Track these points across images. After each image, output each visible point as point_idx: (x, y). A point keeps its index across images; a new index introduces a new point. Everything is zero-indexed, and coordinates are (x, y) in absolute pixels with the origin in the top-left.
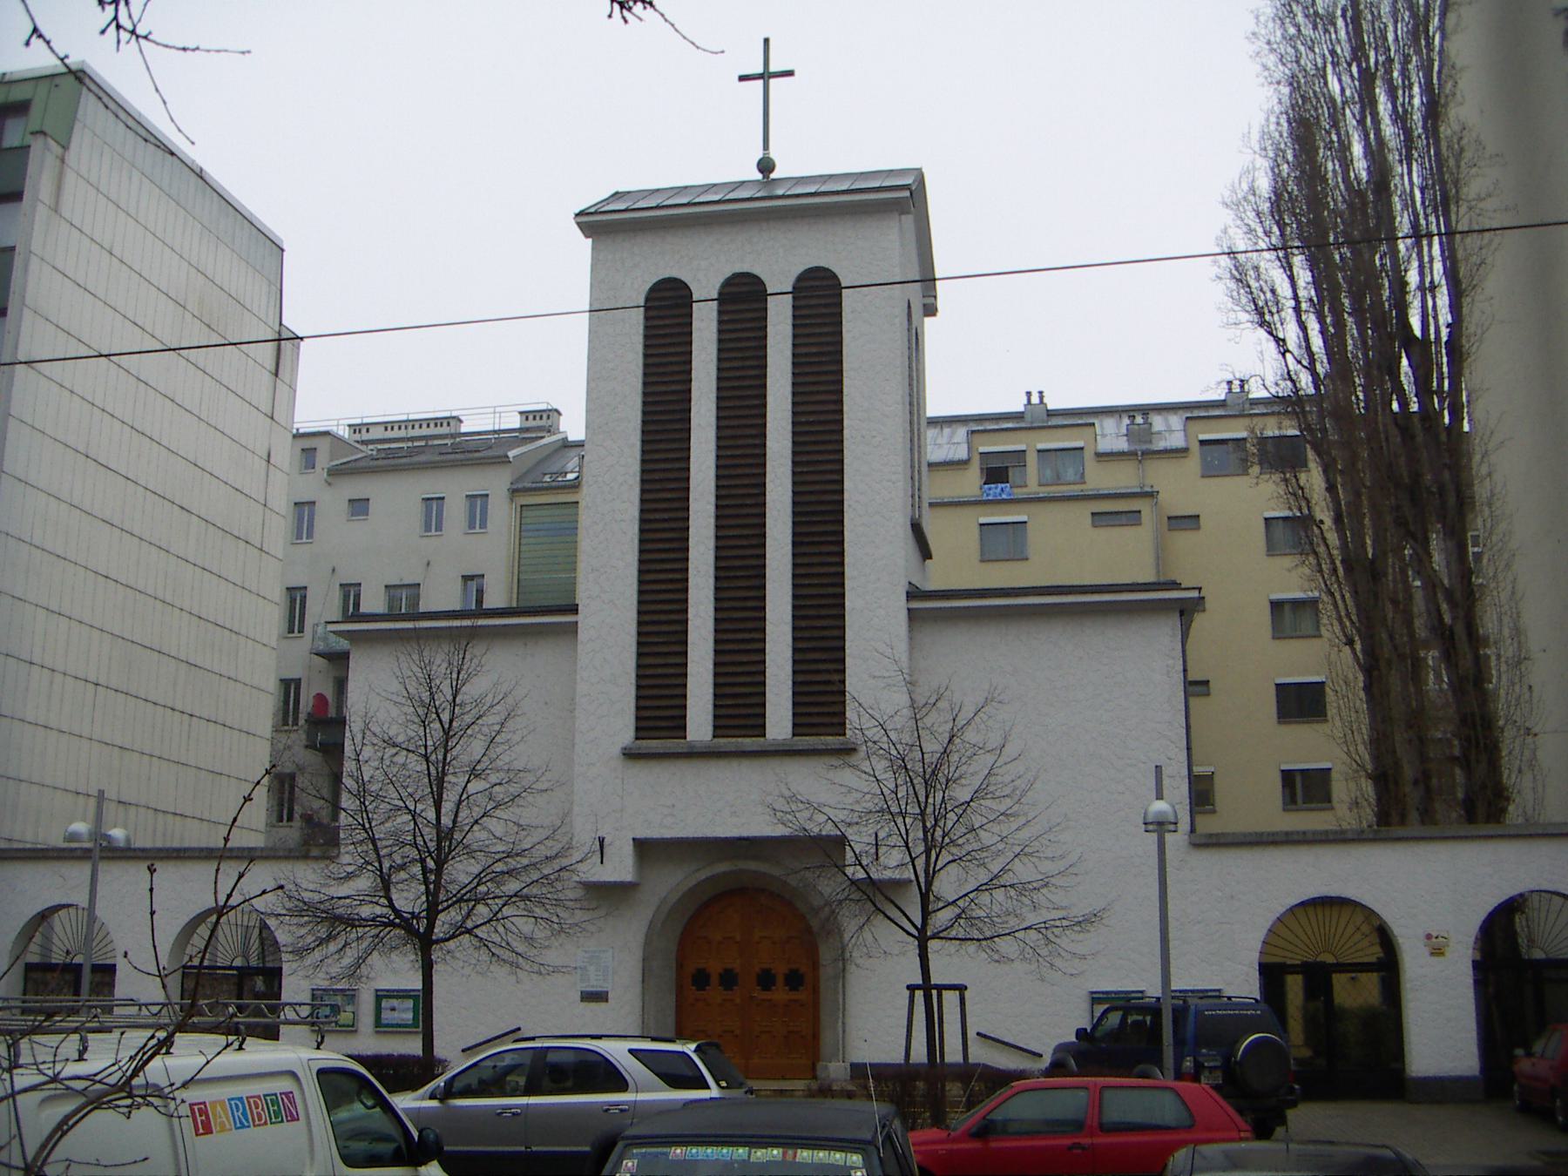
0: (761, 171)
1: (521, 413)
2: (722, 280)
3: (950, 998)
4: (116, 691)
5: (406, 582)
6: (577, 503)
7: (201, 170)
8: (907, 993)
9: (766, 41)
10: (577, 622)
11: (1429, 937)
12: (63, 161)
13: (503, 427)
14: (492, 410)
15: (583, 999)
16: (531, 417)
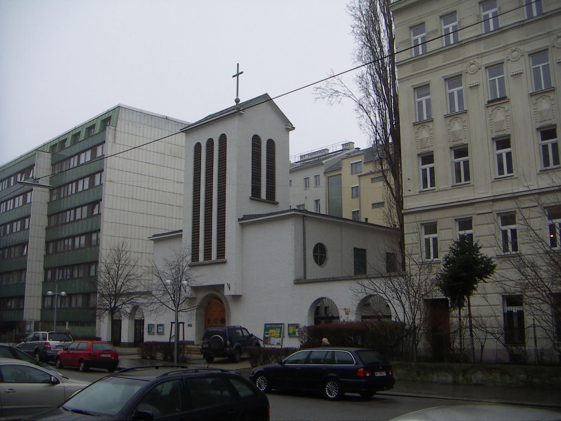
0: (236, 102)
1: (342, 145)
2: (206, 141)
3: (181, 325)
4: (149, 254)
5: (301, 204)
6: (341, 174)
7: (167, 117)
8: (171, 324)
9: (238, 64)
10: (182, 234)
11: (345, 309)
12: (115, 130)
13: (337, 150)
14: (332, 146)
15: (188, 326)
16: (345, 145)
